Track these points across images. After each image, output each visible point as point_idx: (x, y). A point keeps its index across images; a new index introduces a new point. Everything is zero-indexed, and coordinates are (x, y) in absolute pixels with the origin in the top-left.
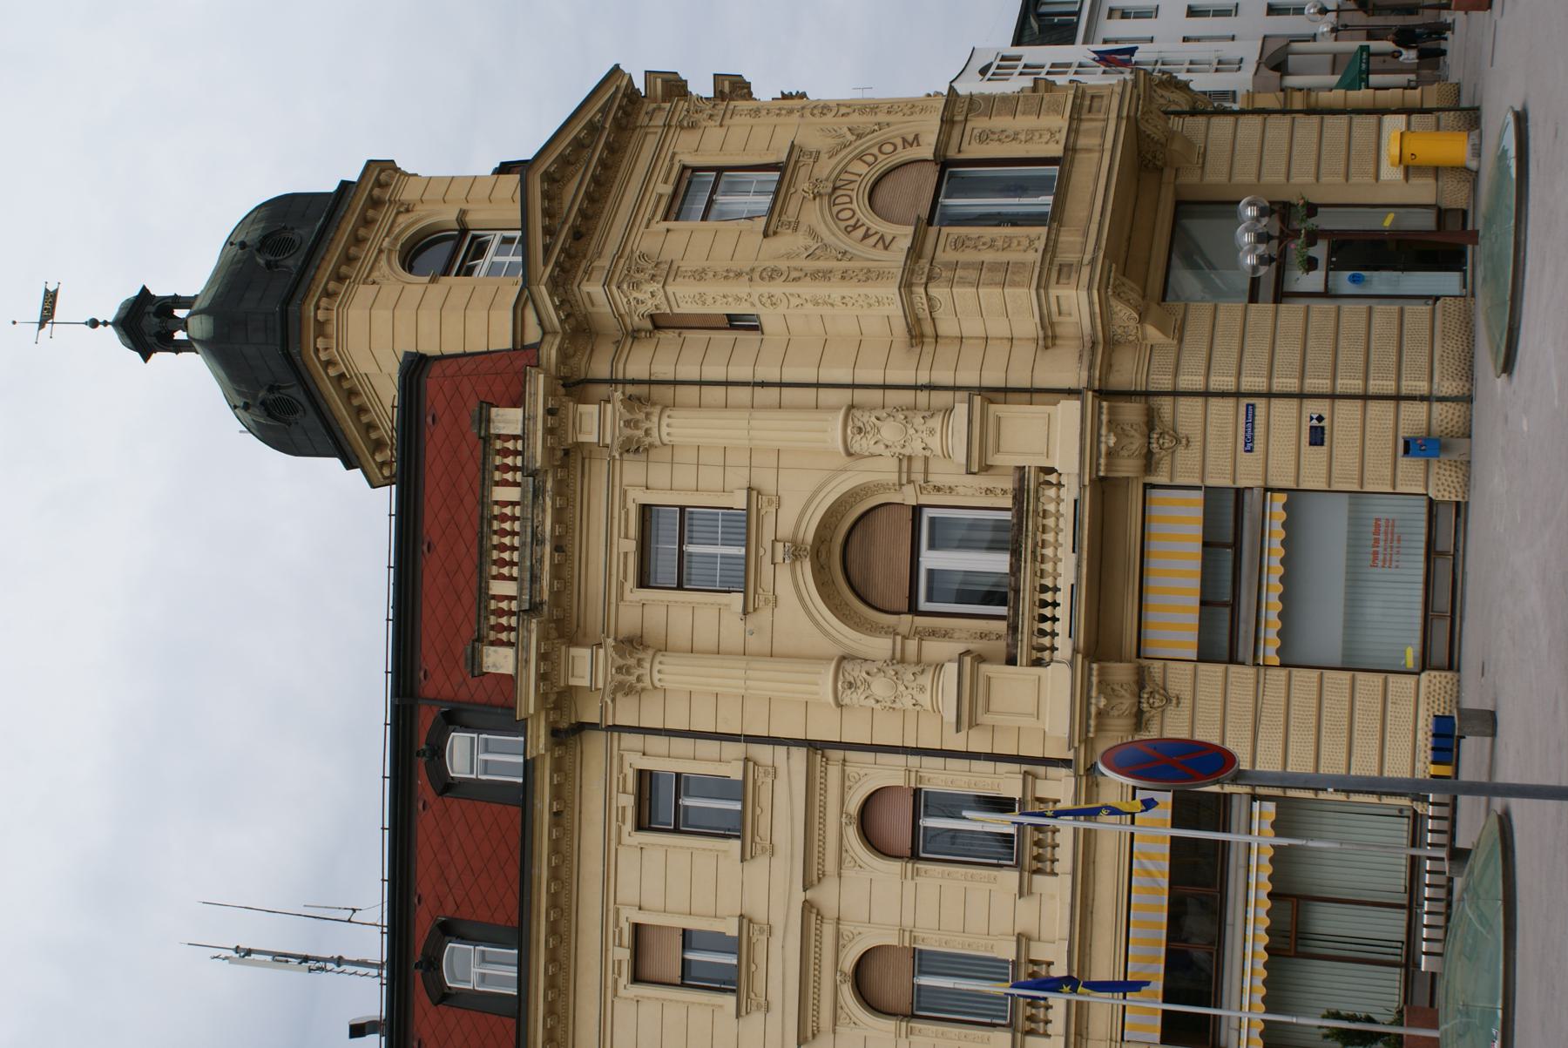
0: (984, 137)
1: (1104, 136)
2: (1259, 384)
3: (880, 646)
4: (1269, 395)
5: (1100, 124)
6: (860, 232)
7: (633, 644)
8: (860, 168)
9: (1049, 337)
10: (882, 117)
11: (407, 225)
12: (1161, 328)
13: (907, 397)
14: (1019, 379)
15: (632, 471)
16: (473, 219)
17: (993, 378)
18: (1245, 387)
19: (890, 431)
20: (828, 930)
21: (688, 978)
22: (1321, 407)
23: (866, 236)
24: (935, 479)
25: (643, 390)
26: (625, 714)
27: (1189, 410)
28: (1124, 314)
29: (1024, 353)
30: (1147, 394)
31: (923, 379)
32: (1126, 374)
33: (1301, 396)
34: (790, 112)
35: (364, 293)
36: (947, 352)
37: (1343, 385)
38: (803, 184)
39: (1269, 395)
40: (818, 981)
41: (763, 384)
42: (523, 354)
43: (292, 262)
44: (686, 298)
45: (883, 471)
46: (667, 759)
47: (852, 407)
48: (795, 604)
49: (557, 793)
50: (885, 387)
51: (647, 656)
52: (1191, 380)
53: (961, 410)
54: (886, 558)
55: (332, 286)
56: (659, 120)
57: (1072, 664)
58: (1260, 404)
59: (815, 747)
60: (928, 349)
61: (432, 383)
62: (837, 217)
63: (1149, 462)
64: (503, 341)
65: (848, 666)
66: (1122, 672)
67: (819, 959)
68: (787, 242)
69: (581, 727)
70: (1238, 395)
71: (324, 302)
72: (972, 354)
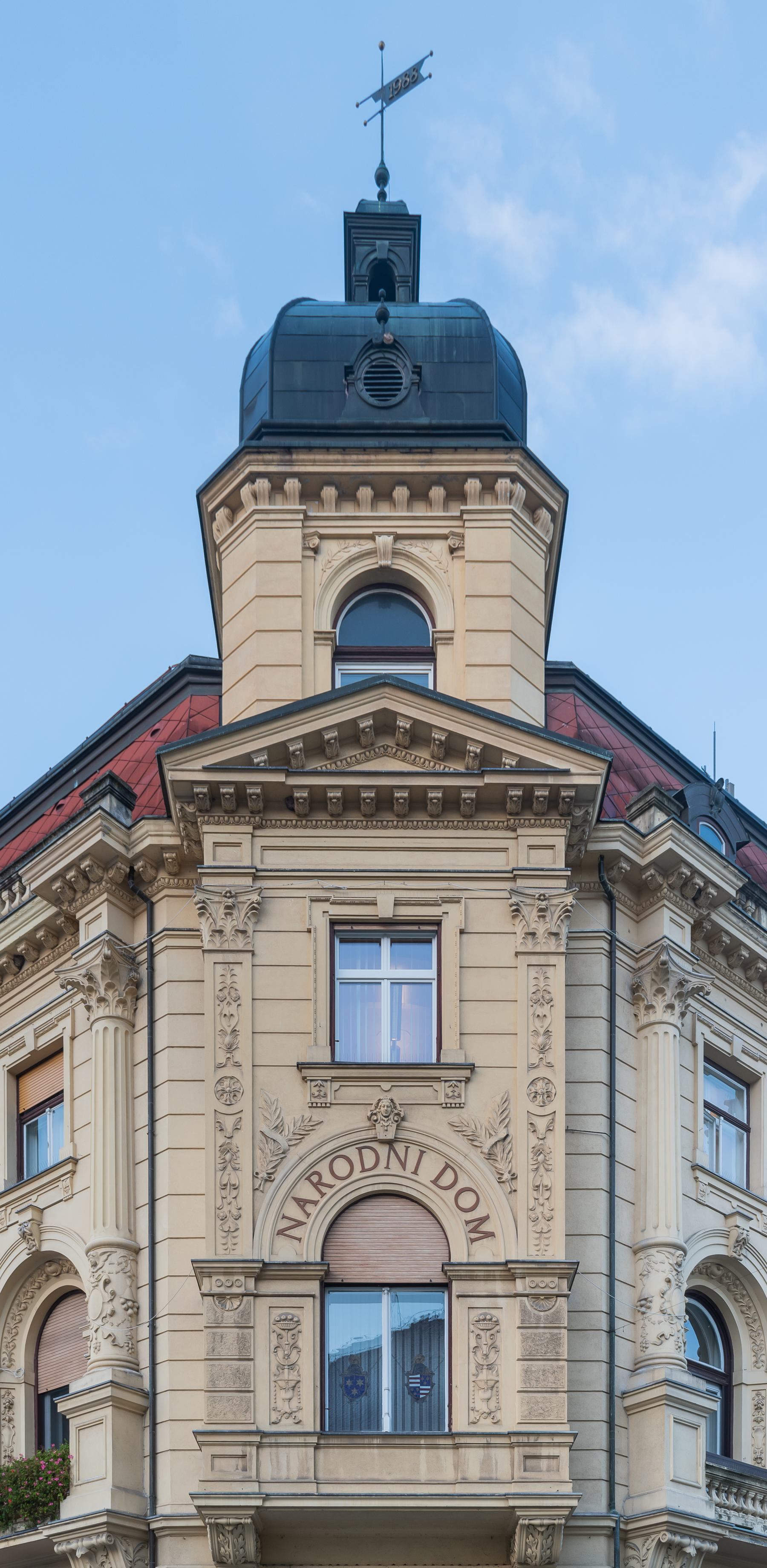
1: (483, 1481)
6: (307, 1191)
8: (431, 1167)
34: (543, 1049)
62: (335, 1155)
68: (292, 1098)
71: (263, 484)
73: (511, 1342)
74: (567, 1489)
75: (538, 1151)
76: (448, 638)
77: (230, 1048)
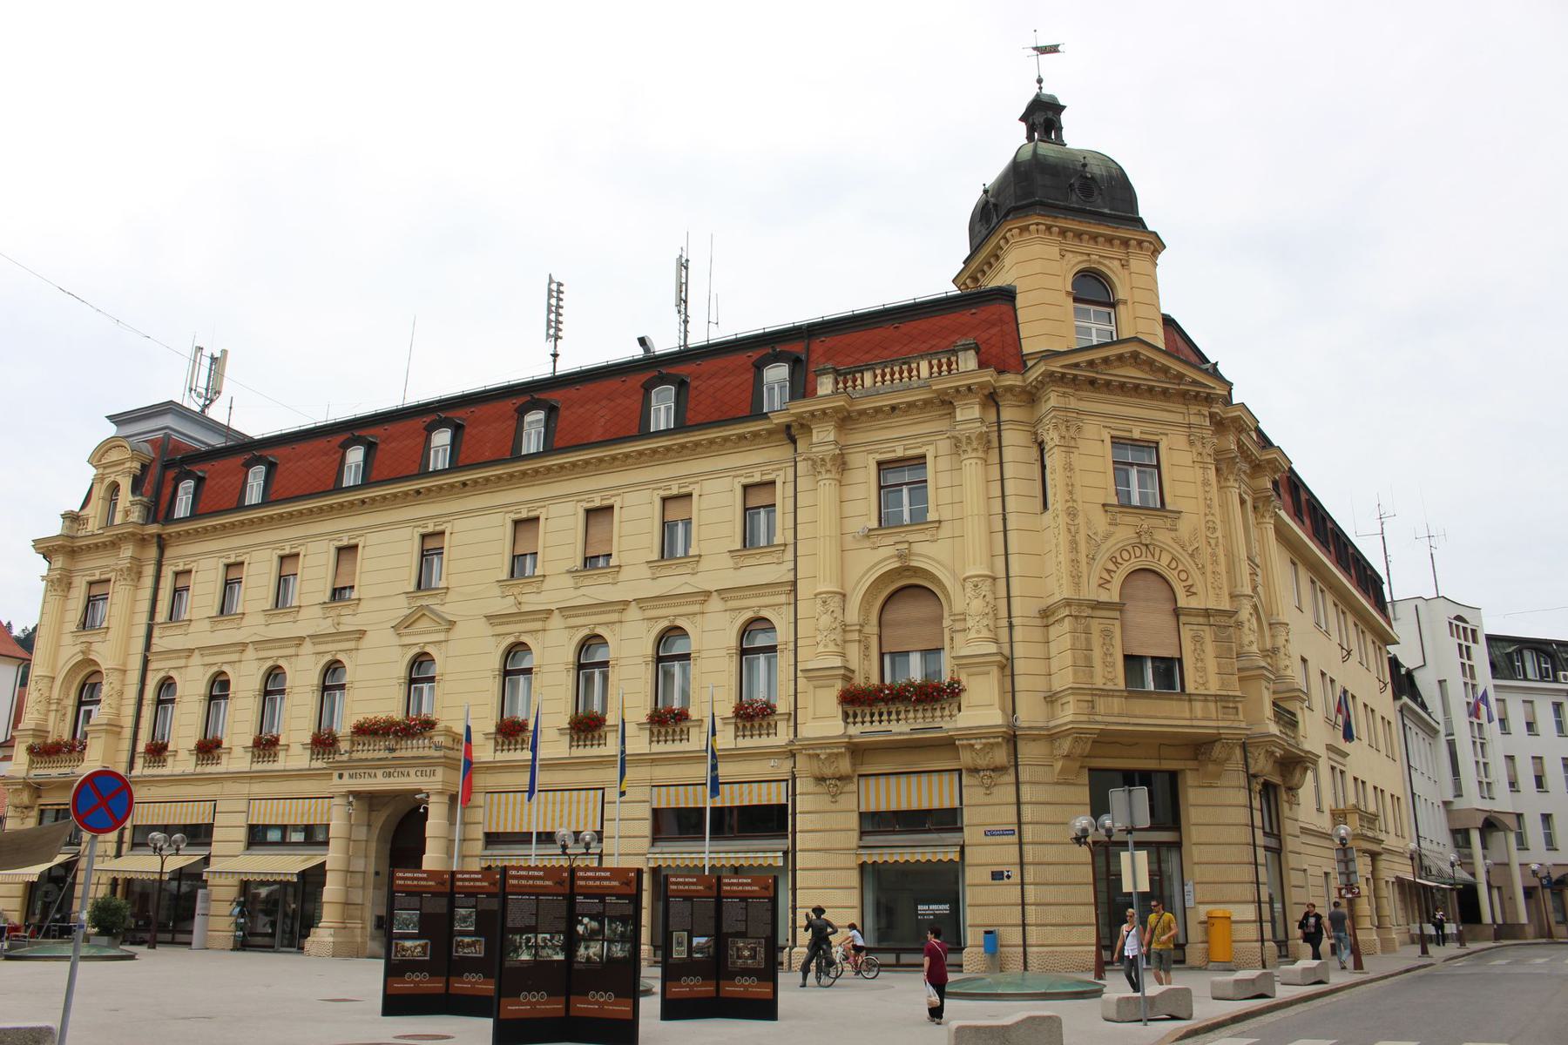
0: (1197, 639)
2: (1027, 837)
3: (853, 616)
4: (1021, 844)
5: (1214, 715)
7: (841, 464)
8: (1165, 559)
9: (1051, 699)
10: (1209, 568)
11: (1112, 268)
12: (1062, 771)
13: (1003, 613)
14: (1020, 683)
15: (944, 446)
16: (1121, 308)
17: (1020, 666)
18: (1024, 827)
19: (977, 605)
20: (696, 608)
21: (667, 527)
22: (1016, 878)
23: (1109, 571)
24: (957, 636)
25: (995, 444)
26: (802, 467)
27: (1008, 793)
28: (1066, 745)
29: (1040, 684)
30: (1016, 766)
31: (1015, 621)
32: (1027, 751)
33: (1022, 864)
35: (1054, 251)
36: (1037, 634)
37: (1029, 890)
38: (1147, 523)
39: (1021, 844)
40: (669, 606)
41: (1004, 520)
42: (1021, 363)
43: (1075, 200)
44: (1054, 460)
45: (958, 606)
46: (782, 495)
47: (994, 579)
48: (876, 560)
49: (756, 435)
50: (1009, 597)
51: (834, 475)
52: (1027, 793)
53: (993, 648)
54: (908, 610)
55: (1055, 230)
56: (1194, 420)
57: (844, 735)
58: (1015, 838)
59: (795, 583)
60: (1038, 622)
61: (1000, 308)
63: (974, 771)
64: (1027, 348)
65: (837, 598)
66: (845, 766)
67: (681, 605)
69: (794, 442)
70: (1020, 823)
72: (1038, 650)
73: (1210, 648)
74: (1243, 725)
75: (1213, 555)
76: (1125, 302)
77: (1071, 493)
